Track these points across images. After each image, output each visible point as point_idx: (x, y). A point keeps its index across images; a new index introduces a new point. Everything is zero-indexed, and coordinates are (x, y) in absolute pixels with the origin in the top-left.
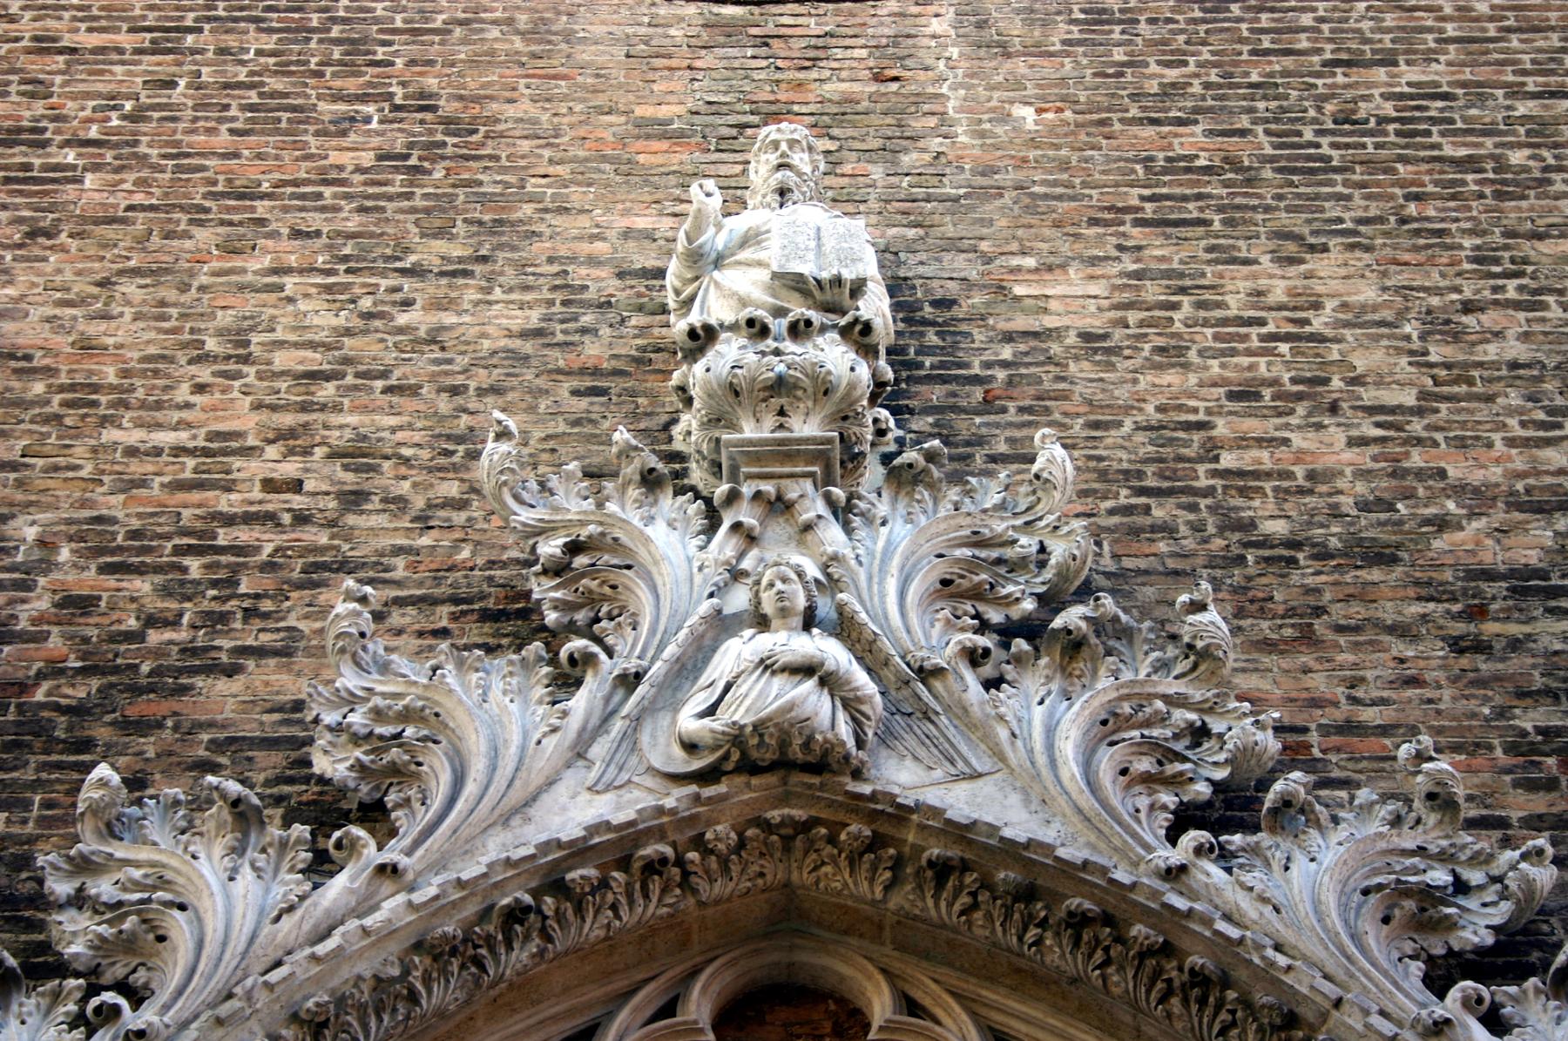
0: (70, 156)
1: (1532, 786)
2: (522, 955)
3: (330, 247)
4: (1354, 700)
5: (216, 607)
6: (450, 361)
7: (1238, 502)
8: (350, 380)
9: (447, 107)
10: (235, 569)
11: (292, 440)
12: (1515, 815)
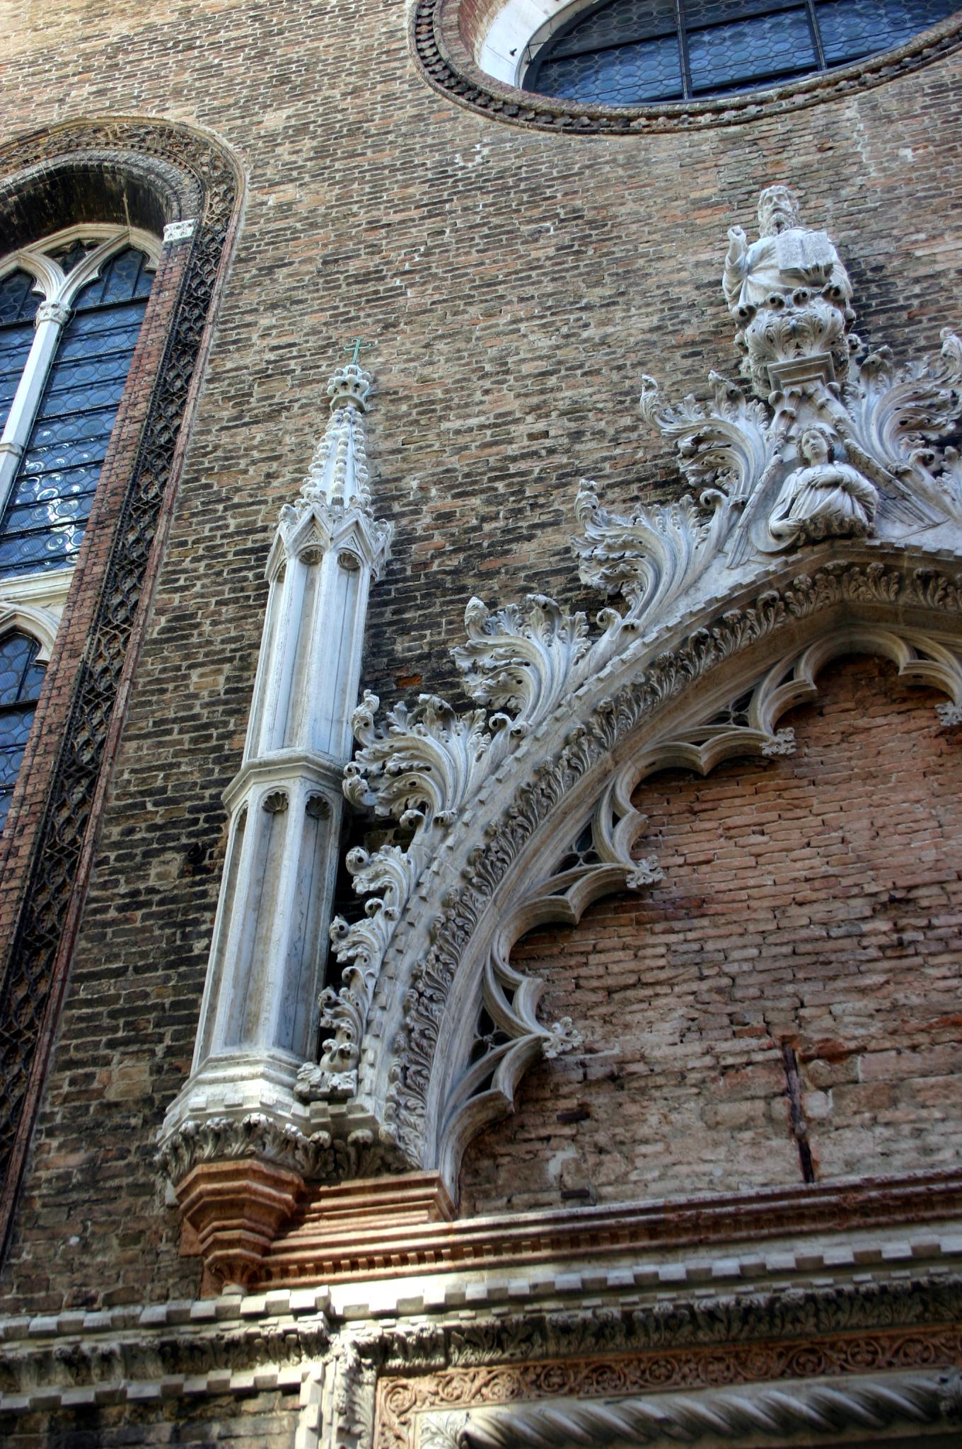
0: (398, 282)
2: (707, 661)
5: (516, 506)
8: (563, 373)
9: (589, 215)
10: (522, 484)
11: (539, 410)
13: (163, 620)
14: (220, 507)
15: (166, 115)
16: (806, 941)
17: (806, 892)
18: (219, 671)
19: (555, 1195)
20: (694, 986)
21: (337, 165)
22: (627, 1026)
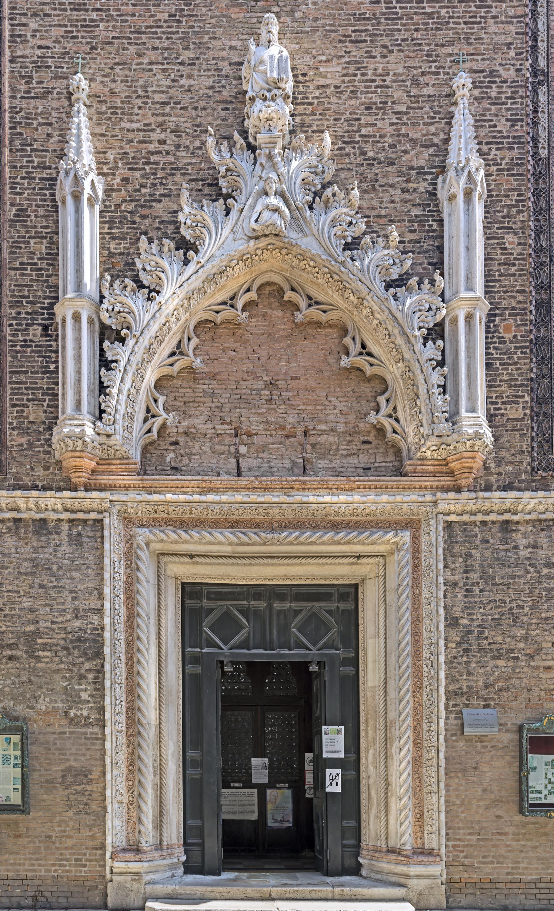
1: (412, 231)
3: (162, 53)
4: (381, 208)
5: (153, 181)
6: (193, 98)
7: (364, 146)
12: (407, 240)
14: (29, 149)
16: (245, 394)
17: (245, 376)
18: (42, 243)
19: (169, 468)
20: (210, 405)
22: (190, 416)
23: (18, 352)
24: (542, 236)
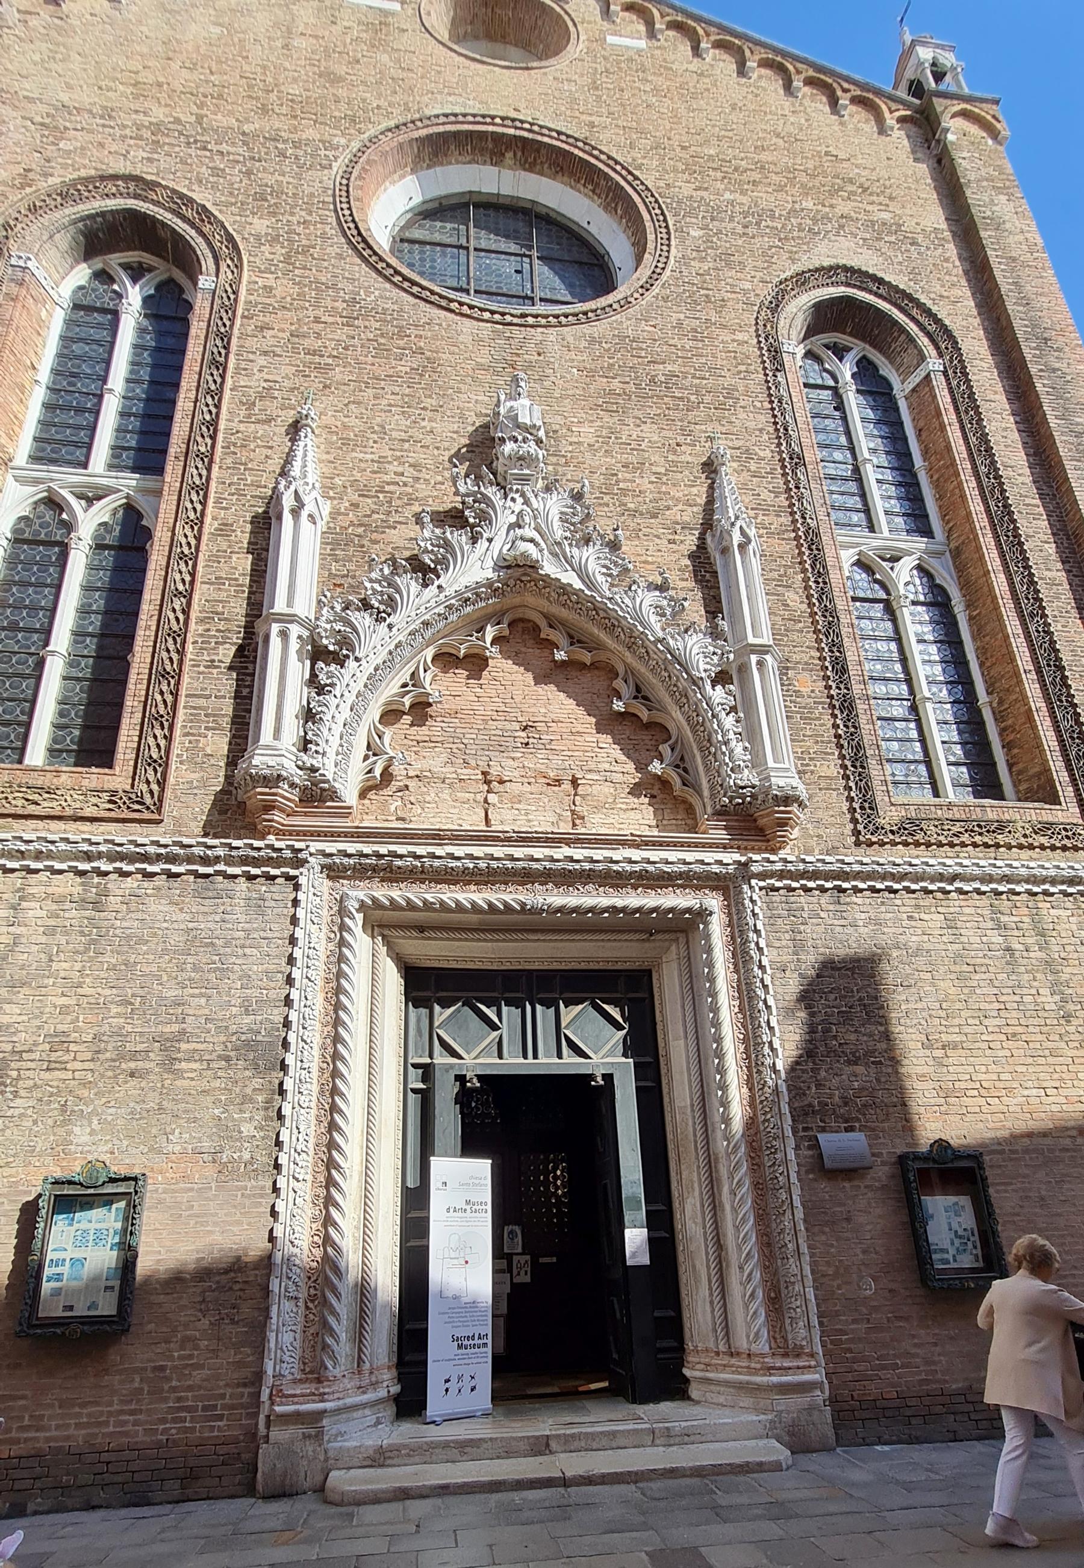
0: (330, 361)
1: (683, 580)
13: (216, 524)
14: (242, 467)
15: (194, 196)
20: (451, 746)
21: (297, 272)
23: (199, 673)
24: (824, 597)
